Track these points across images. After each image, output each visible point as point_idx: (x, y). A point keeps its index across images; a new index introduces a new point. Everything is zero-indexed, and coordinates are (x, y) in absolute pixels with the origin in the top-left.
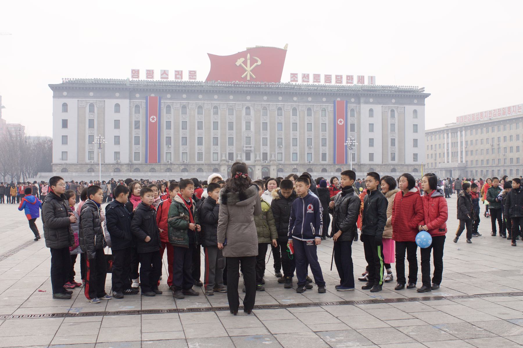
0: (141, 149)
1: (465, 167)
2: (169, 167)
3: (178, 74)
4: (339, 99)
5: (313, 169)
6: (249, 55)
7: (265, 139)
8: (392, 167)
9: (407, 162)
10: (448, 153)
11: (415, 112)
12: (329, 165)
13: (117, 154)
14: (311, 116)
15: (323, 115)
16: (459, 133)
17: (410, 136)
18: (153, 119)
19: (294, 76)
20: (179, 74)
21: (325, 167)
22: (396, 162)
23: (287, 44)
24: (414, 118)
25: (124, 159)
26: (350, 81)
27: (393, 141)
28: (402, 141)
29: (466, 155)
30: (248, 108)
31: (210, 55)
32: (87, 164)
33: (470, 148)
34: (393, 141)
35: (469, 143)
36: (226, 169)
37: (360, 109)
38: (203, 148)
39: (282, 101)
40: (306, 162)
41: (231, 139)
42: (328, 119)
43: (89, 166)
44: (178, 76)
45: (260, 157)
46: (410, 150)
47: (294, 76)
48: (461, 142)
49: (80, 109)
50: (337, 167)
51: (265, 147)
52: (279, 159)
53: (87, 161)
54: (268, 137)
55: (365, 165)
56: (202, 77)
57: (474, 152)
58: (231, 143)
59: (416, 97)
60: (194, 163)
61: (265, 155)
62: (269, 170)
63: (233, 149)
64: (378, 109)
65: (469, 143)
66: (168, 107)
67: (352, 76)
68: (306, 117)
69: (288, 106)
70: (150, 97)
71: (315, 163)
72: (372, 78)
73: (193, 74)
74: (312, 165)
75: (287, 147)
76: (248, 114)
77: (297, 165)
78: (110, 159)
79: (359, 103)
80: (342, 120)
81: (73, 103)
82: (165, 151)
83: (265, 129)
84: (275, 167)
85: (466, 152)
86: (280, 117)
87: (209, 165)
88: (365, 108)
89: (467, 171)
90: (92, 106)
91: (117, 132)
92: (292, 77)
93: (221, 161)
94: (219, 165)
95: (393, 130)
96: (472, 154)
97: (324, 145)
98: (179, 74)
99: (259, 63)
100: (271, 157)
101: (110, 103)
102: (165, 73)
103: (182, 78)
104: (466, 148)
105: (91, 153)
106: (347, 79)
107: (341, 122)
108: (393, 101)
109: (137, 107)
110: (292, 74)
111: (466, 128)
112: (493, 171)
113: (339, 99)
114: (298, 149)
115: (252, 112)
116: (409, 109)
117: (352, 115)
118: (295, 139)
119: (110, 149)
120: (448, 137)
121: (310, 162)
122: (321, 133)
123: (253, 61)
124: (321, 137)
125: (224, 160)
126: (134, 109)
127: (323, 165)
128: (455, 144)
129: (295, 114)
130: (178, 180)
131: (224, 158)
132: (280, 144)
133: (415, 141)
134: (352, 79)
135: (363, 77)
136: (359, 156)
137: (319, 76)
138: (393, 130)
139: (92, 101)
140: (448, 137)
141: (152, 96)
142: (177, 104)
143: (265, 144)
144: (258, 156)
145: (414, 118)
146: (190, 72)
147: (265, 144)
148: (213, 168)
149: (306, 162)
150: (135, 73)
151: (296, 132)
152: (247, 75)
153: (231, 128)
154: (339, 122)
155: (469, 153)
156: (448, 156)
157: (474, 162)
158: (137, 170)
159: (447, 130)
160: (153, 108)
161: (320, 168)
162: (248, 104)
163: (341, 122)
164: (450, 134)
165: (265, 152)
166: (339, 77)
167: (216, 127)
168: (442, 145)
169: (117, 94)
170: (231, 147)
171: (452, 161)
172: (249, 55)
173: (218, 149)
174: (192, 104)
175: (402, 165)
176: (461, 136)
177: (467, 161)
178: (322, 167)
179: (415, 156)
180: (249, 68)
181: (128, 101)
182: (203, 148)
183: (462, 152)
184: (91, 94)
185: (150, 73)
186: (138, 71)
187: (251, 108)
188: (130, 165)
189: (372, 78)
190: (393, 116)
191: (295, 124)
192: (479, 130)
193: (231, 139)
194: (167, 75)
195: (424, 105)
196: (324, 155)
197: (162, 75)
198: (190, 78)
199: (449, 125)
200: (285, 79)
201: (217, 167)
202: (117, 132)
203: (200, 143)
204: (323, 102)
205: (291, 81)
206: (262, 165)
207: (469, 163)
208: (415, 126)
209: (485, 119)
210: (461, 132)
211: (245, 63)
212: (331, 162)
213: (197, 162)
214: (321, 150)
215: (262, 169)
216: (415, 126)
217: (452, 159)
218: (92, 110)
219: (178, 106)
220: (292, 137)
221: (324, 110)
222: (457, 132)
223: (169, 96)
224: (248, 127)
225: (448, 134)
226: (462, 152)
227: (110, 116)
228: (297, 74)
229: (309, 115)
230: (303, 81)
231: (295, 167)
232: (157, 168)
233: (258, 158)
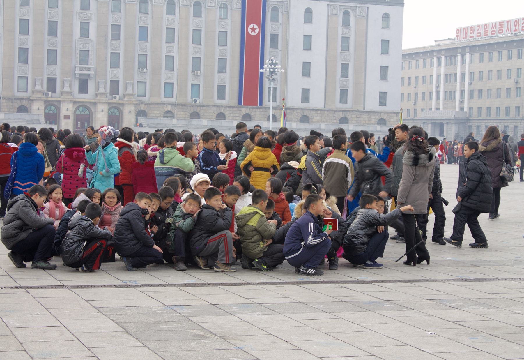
1: (468, 120)
5: (201, 113)
7: (115, 56)
8: (341, 115)
9: (368, 108)
10: (438, 93)
11: (386, 17)
12: (230, 107)
14: (200, 16)
16: (459, 58)
17: (375, 59)
21: (222, 110)
22: (348, 106)
24: (383, 28)
27: (345, 68)
28: (361, 69)
29: (471, 96)
33: (478, 85)
34: (345, 68)
35: (476, 76)
36: (43, 108)
40: (189, 100)
41: (52, 54)
45: (105, 88)
46: (374, 86)
48: (463, 74)
52: (141, 92)
55: (293, 109)
57: (484, 94)
61: (115, 84)
62: (121, 112)
63: (57, 73)
65: (476, 76)
71: (205, 103)
77: (172, 104)
80: (256, 26)
83: (116, 36)
84: (133, 108)
85: (471, 92)
86: (143, 16)
87: (10, 99)
89: (470, 127)
93: (33, 92)
94: (30, 100)
95: (345, 48)
96: (480, 96)
97: (222, 69)
100: (126, 88)
104: (470, 84)
107: (253, 30)
111: (472, 49)
112: (516, 127)
117: (275, 19)
118: (170, 59)
120: (439, 65)
121: (195, 101)
122: (217, 48)
124: (217, 57)
125: (39, 91)
127: (218, 107)
128: (450, 77)
130: (178, 130)
131: (38, 88)
132: (142, 65)
136: (284, 91)
138: (345, 48)
140: (439, 65)
144: (102, 86)
145: (383, 28)
147: (115, 64)
148: (17, 105)
149: (189, 100)
153: (53, 31)
154: (250, 31)
155: (476, 94)
156: (438, 98)
157: (484, 111)
159: (439, 51)
161: (213, 112)
163: (253, 30)
164: (443, 59)
165: (115, 79)
168: (428, 79)
170: (52, 68)
171: (444, 108)
173: (29, 70)
175: (359, 111)
176: (463, 62)
177: (470, 109)
178: (217, 111)
179: (383, 98)
183: (462, 92)
190: (346, 23)
191: (171, 31)
192: (496, 54)
193: (52, 54)
195: (402, 5)
196: (221, 90)
199: (441, 43)
201: (25, 103)
206: (109, 104)
207: (475, 112)
208: (385, 43)
209: (507, 35)
210: (463, 55)
212: (235, 102)
214: (217, 79)
215: (109, 110)
216: (385, 43)
217: (444, 104)
220: (164, 54)
222: (456, 56)
225: (439, 59)
226: (462, 92)
229: (197, 14)
231: (169, 108)
233: (101, 90)
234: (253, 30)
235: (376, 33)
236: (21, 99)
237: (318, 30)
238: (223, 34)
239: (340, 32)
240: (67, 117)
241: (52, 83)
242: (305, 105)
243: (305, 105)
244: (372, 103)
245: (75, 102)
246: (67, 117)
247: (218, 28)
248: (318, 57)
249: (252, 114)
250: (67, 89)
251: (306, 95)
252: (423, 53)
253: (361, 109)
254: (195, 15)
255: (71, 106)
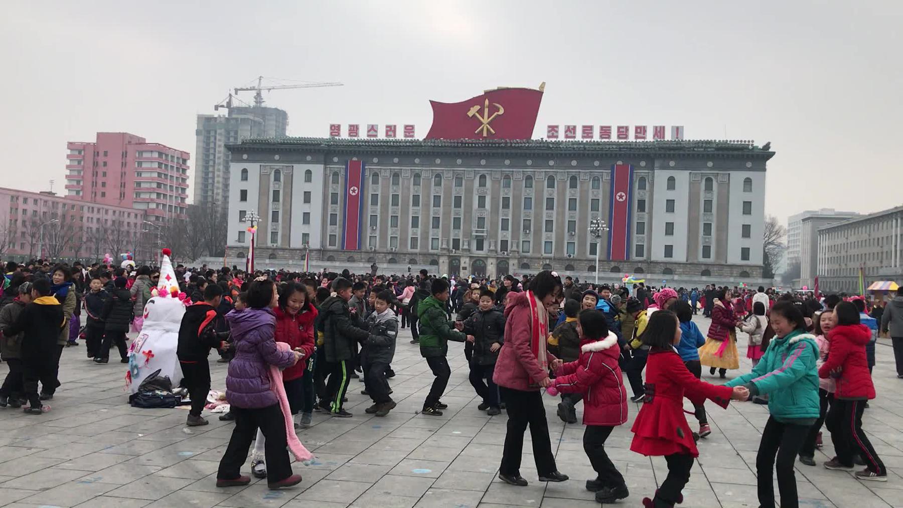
0: (337, 230)
2: (372, 255)
3: (391, 130)
4: (620, 163)
6: (487, 102)
7: (505, 222)
8: (703, 268)
11: (748, 181)
13: (305, 236)
15: (595, 187)
17: (736, 219)
18: (354, 191)
19: (553, 129)
20: (391, 129)
22: (712, 259)
23: (544, 83)
25: (315, 243)
26: (642, 135)
28: (723, 228)
30: (483, 177)
31: (432, 103)
32: (268, 248)
37: (653, 177)
38: (419, 231)
39: (532, 166)
41: (457, 221)
42: (601, 194)
43: (270, 252)
44: (390, 133)
47: (553, 129)
49: (263, 177)
50: (613, 264)
51: (505, 233)
53: (269, 244)
54: (510, 218)
55: (657, 263)
56: (421, 134)
58: (457, 226)
59: (754, 158)
60: (405, 251)
61: (504, 243)
64: (683, 177)
66: (376, 175)
67: (644, 127)
68: (568, 190)
69: (540, 175)
70: (351, 161)
72: (677, 130)
73: (409, 129)
74: (574, 260)
75: (538, 233)
76: (482, 184)
77: (550, 259)
78: (296, 242)
79: (653, 169)
80: (623, 194)
81: (254, 169)
82: (369, 235)
83: (506, 205)
84: (516, 261)
88: (661, 176)
90: (277, 172)
91: (306, 208)
92: (549, 132)
98: (391, 129)
99: (501, 111)
101: (299, 170)
102: (372, 129)
103: (395, 136)
105: (274, 234)
106: (636, 132)
107: (621, 197)
108: (710, 164)
109: (336, 174)
110: (549, 127)
113: (620, 163)
114: (553, 236)
115: (489, 183)
116: (737, 177)
117: (642, 187)
118: (549, 223)
119: (298, 229)
120: (897, 226)
123: (492, 110)
125: (444, 249)
126: (331, 178)
129: (551, 185)
132: (527, 227)
133: (242, 213)
134: (645, 131)
135: (662, 129)
137: (591, 128)
139: (278, 166)
140: (897, 226)
141: (352, 158)
142: (385, 172)
143: (505, 228)
146: (406, 127)
149: (566, 255)
150: (335, 129)
151: (550, 211)
152: (482, 130)
153: (458, 204)
158: (331, 259)
160: (355, 178)
161: (586, 265)
162: (482, 171)
163: (621, 197)
164: (899, 221)
166: (624, 130)
167: (437, 204)
169: (309, 158)
170: (456, 231)
172: (487, 102)
174: (406, 171)
180: (485, 120)
181: (322, 166)
182: (419, 231)
184: (277, 157)
185: (354, 129)
186: (339, 126)
187: (487, 177)
188: (322, 253)
189: (677, 130)
190: (709, 188)
193: (457, 221)
194: (376, 131)
195: (765, 170)
197: (369, 131)
198: (406, 136)
200: (539, 133)
202: (306, 208)
203: (415, 224)
204: (596, 168)
205: (549, 137)
211: (481, 112)
213: (410, 250)
218: (277, 179)
219: (388, 174)
220: (545, 218)
221: (596, 180)
223: (375, 160)
224: (482, 204)
227: (300, 186)
228: (557, 127)
230: (567, 137)
232: (356, 256)
234: (621, 197)
235: (737, 196)
236: (412, 254)
237: (681, 195)
238: (595, 202)
239: (703, 197)
240: (465, 268)
241: (456, 243)
242: (668, 259)
243: (668, 259)
244: (734, 258)
245: (471, 257)
246: (465, 268)
247: (591, 197)
248: (680, 217)
249: (621, 267)
250: (466, 247)
251: (669, 250)
252: (882, 216)
253: (724, 263)
254: (571, 187)
255: (467, 260)
